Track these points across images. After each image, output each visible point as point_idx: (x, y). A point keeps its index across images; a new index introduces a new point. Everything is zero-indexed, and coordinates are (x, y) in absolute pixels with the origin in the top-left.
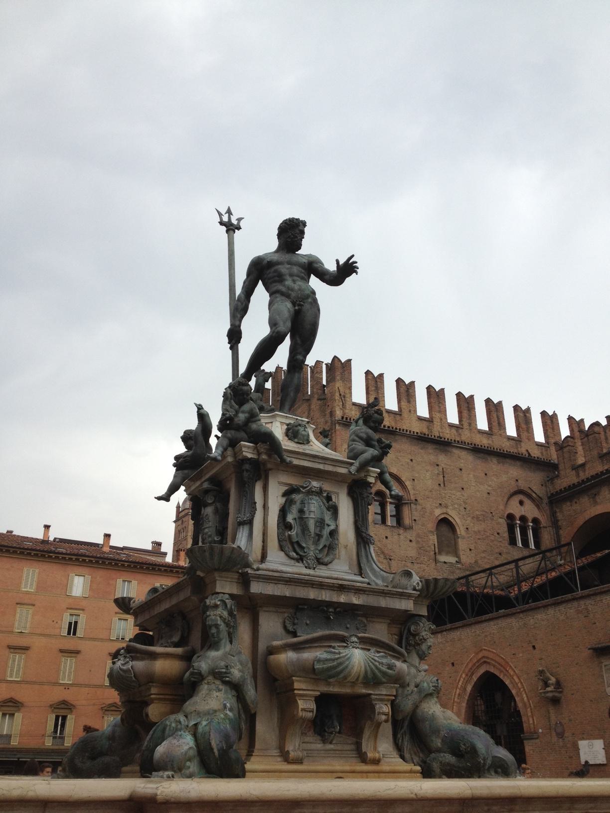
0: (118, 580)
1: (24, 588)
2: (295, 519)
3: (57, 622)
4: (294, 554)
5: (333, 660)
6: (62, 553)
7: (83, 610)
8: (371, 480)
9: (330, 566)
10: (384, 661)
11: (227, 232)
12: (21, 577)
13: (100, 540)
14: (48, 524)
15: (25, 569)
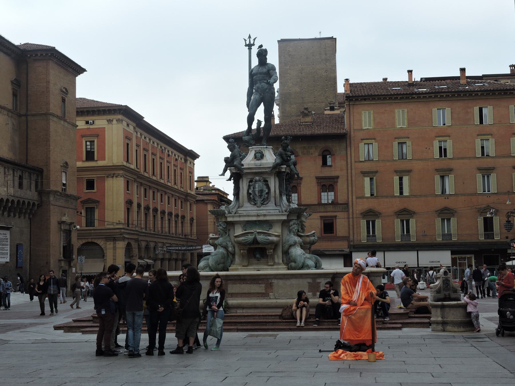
0: (475, 108)
1: (398, 126)
2: (252, 191)
3: (429, 149)
4: (253, 203)
5: (247, 239)
6: (422, 93)
7: (450, 136)
8: (283, 170)
9: (267, 205)
10: (265, 238)
11: (248, 49)
12: (394, 118)
13: (458, 74)
14: (411, 69)
15: (396, 111)
